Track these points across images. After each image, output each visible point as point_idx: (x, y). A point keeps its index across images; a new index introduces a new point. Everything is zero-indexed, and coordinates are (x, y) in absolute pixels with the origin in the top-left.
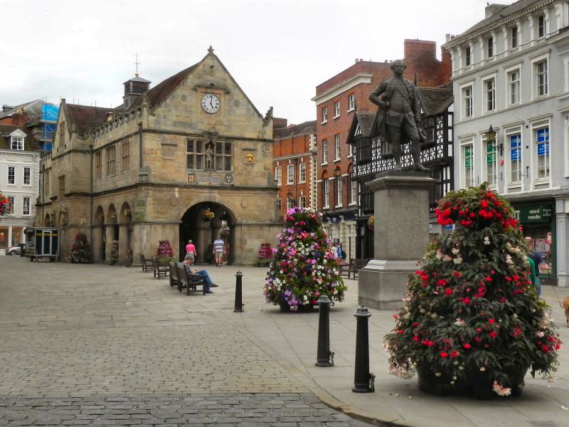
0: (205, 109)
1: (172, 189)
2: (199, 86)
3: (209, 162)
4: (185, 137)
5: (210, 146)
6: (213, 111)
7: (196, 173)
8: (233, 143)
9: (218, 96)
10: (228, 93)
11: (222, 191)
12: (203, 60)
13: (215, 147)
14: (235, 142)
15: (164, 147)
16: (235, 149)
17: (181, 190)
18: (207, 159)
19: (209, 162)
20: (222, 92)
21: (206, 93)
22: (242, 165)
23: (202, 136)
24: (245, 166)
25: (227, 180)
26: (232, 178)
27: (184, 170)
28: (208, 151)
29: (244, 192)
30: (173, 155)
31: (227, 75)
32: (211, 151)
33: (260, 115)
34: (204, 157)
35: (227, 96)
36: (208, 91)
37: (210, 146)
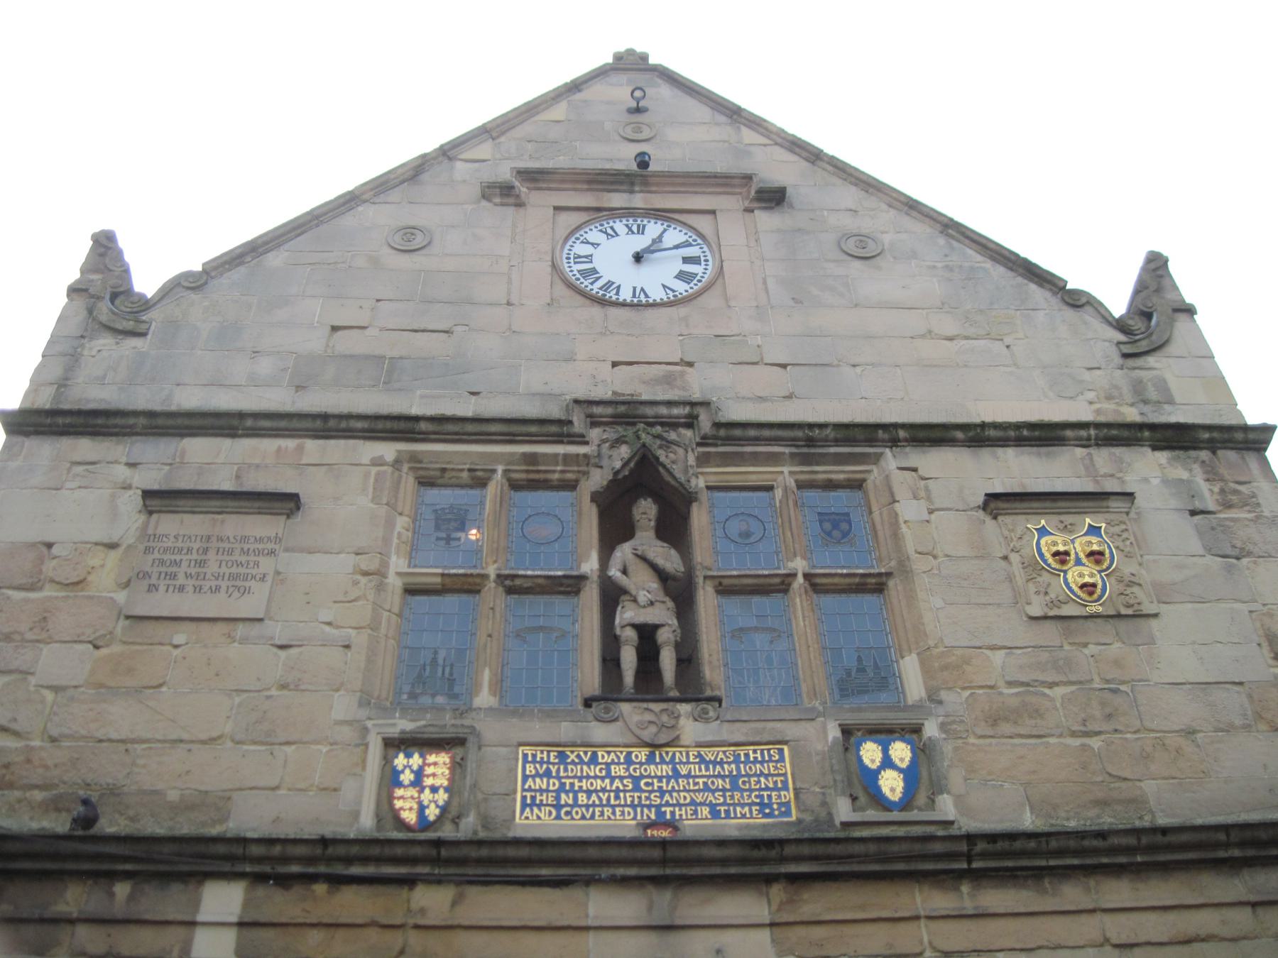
0: (595, 288)
1: (167, 902)
2: (534, 177)
3: (647, 634)
4: (388, 450)
5: (646, 510)
6: (657, 294)
7: (490, 730)
8: (874, 476)
9: (703, 223)
10: (774, 198)
11: (816, 902)
12: (575, 87)
13: (699, 518)
14: (891, 460)
15: (169, 525)
16: (909, 510)
17: (281, 904)
18: (626, 614)
19: (647, 634)
20: (729, 204)
21: (600, 213)
22: (1023, 634)
23: (556, 430)
24: (1050, 633)
25: (871, 777)
26: (923, 752)
27: (343, 706)
28: (624, 552)
29: (1119, 892)
30: (239, 583)
31: (749, 136)
32: (669, 559)
33: (1077, 301)
34: (591, 596)
35: (766, 220)
36: (617, 200)
37: (646, 510)
